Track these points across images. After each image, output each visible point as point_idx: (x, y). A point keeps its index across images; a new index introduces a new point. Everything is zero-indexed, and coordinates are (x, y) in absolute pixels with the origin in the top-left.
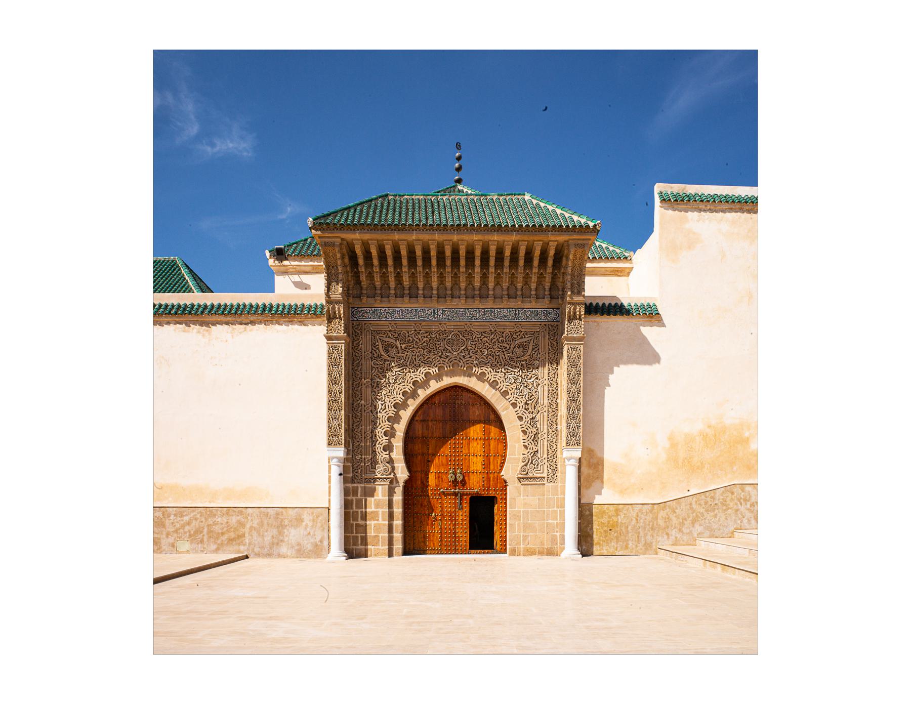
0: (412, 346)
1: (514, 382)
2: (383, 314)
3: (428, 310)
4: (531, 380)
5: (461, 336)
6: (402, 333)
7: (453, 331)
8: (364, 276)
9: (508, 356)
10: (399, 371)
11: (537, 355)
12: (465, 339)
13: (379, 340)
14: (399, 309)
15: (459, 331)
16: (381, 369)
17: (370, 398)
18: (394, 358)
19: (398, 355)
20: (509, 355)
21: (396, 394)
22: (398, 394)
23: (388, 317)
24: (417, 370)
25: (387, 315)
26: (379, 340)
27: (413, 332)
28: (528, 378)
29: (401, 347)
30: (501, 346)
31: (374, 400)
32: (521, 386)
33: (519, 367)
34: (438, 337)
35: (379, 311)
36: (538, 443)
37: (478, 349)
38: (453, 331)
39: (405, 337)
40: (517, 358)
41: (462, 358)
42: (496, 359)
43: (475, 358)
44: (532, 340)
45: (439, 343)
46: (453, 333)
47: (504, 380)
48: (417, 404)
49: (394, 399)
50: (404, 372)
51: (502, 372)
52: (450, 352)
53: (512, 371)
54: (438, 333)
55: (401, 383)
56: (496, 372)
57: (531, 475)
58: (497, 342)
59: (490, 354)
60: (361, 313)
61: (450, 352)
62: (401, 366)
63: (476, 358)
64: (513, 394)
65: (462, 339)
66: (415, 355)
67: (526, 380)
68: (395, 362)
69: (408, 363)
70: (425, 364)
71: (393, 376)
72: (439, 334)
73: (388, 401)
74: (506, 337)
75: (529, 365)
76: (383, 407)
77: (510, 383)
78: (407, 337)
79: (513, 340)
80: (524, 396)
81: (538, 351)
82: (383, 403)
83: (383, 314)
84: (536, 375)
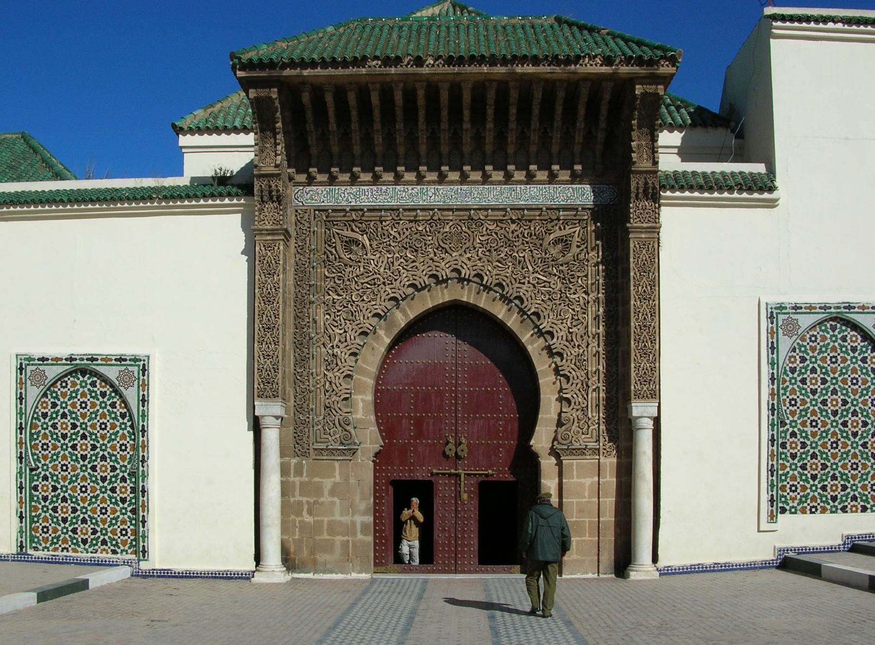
0: (388, 243)
1: (549, 299)
2: (343, 195)
3: (412, 189)
4: (577, 296)
5: (464, 228)
6: (372, 223)
7: (451, 220)
8: (314, 138)
9: (539, 258)
10: (367, 283)
11: (585, 256)
12: (470, 233)
13: (336, 236)
14: (368, 187)
15: (460, 220)
16: (340, 280)
17: (322, 323)
18: (359, 262)
19: (365, 256)
20: (539, 256)
21: (362, 319)
22: (366, 318)
23: (350, 200)
24: (396, 280)
25: (349, 198)
26: (336, 236)
27: (388, 222)
28: (572, 291)
29: (371, 245)
30: (527, 243)
31: (328, 327)
32: (560, 304)
33: (555, 275)
34: (428, 230)
35: (337, 192)
36: (587, 395)
37: (491, 247)
38: (451, 220)
39: (377, 229)
40: (553, 260)
41: (465, 262)
42: (520, 262)
43: (486, 261)
44: (577, 233)
45: (430, 238)
46: (451, 223)
47: (533, 296)
48: (396, 332)
49: (360, 326)
50: (375, 284)
51: (529, 282)
52: (446, 252)
53: (545, 282)
54: (429, 222)
55: (370, 301)
56: (520, 283)
57: (576, 445)
58: (520, 236)
59: (511, 255)
60: (309, 195)
61: (446, 252)
62: (370, 274)
63: (488, 261)
64: (547, 317)
65: (465, 232)
66: (393, 257)
67: (568, 295)
68: (362, 269)
69: (382, 270)
70: (408, 271)
71: (358, 290)
72: (430, 224)
73: (351, 329)
74: (535, 228)
75: (571, 271)
76: (343, 340)
77: (543, 300)
78: (380, 229)
79: (546, 233)
80: (565, 321)
81: (585, 250)
82: (342, 332)
83: (343, 195)
84: (584, 288)
